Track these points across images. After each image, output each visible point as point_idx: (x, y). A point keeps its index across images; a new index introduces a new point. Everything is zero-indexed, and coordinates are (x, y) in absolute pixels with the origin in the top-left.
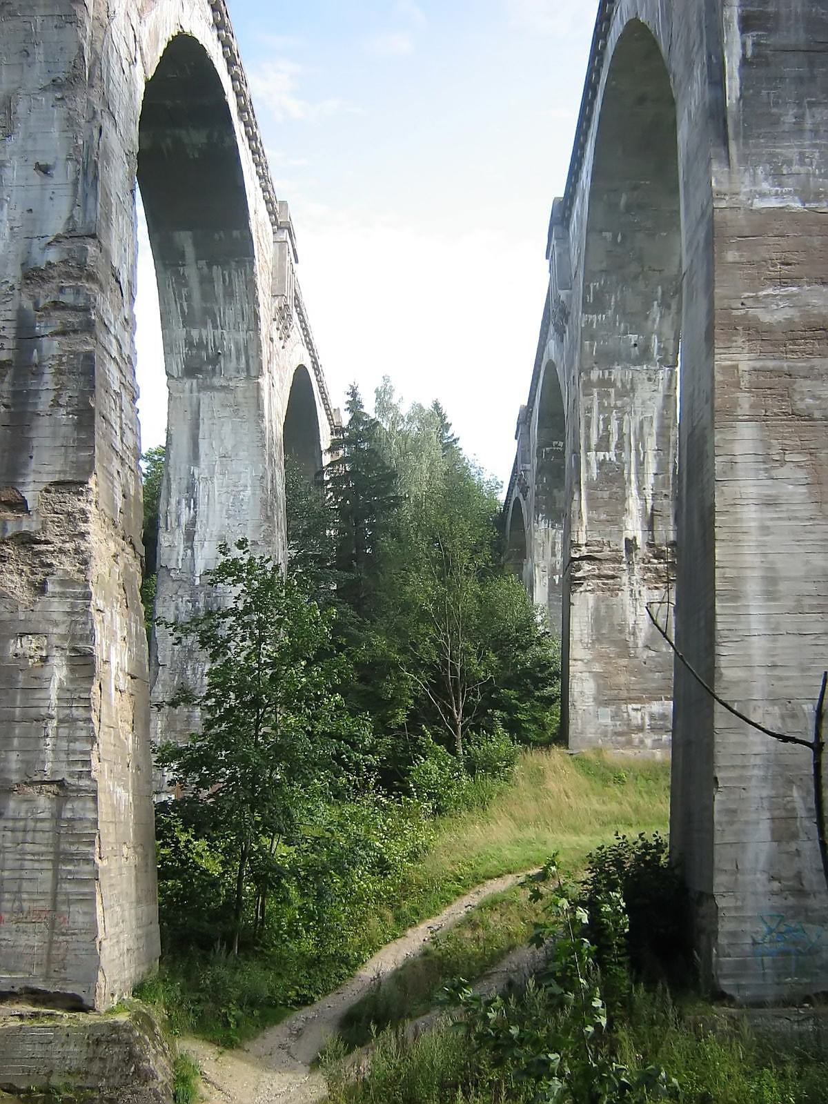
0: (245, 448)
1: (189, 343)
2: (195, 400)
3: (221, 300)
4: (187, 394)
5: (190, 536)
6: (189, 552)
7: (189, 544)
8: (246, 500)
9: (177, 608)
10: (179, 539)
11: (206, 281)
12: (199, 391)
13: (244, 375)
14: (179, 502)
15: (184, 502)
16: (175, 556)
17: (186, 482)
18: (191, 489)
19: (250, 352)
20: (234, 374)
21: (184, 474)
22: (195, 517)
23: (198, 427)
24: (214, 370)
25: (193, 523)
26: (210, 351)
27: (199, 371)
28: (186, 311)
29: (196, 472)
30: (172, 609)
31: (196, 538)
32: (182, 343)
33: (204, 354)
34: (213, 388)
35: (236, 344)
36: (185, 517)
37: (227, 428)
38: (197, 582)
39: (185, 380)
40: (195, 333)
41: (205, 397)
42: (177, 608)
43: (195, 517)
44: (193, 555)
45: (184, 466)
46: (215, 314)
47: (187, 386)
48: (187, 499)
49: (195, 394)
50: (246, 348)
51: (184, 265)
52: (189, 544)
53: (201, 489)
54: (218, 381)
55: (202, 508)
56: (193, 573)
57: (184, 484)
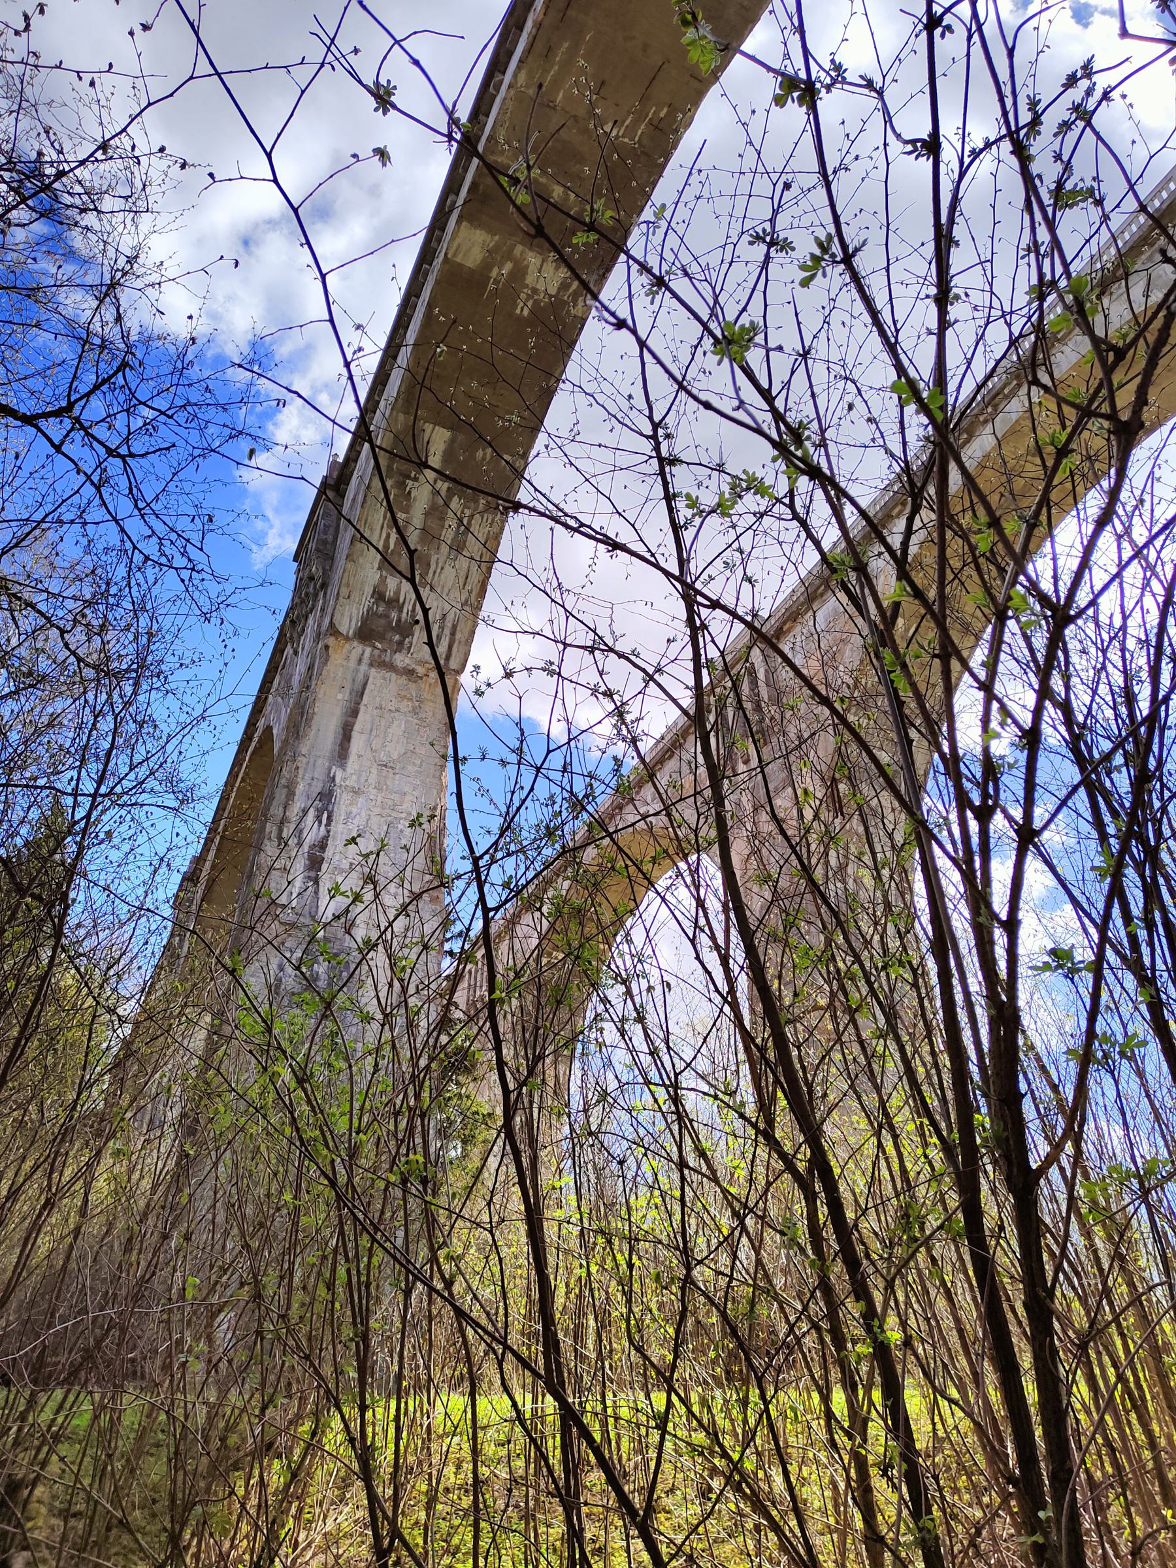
0: (418, 762)
1: (379, 595)
2: (361, 676)
3: (444, 549)
5: (315, 863)
7: (313, 874)
11: (436, 512)
12: (371, 665)
14: (305, 812)
15: (312, 813)
17: (320, 785)
18: (326, 797)
19: (458, 636)
21: (320, 773)
22: (326, 838)
23: (354, 713)
24: (400, 644)
25: (322, 845)
26: (404, 615)
27: (381, 638)
28: (392, 546)
31: (325, 866)
32: (369, 590)
33: (394, 615)
34: (390, 667)
36: (313, 832)
37: (397, 728)
39: (355, 643)
43: (326, 838)
45: (322, 763)
46: (429, 565)
47: (355, 655)
48: (317, 810)
49: (364, 667)
50: (454, 627)
51: (416, 479)
52: (313, 874)
53: (343, 803)
54: (401, 660)
57: (317, 787)
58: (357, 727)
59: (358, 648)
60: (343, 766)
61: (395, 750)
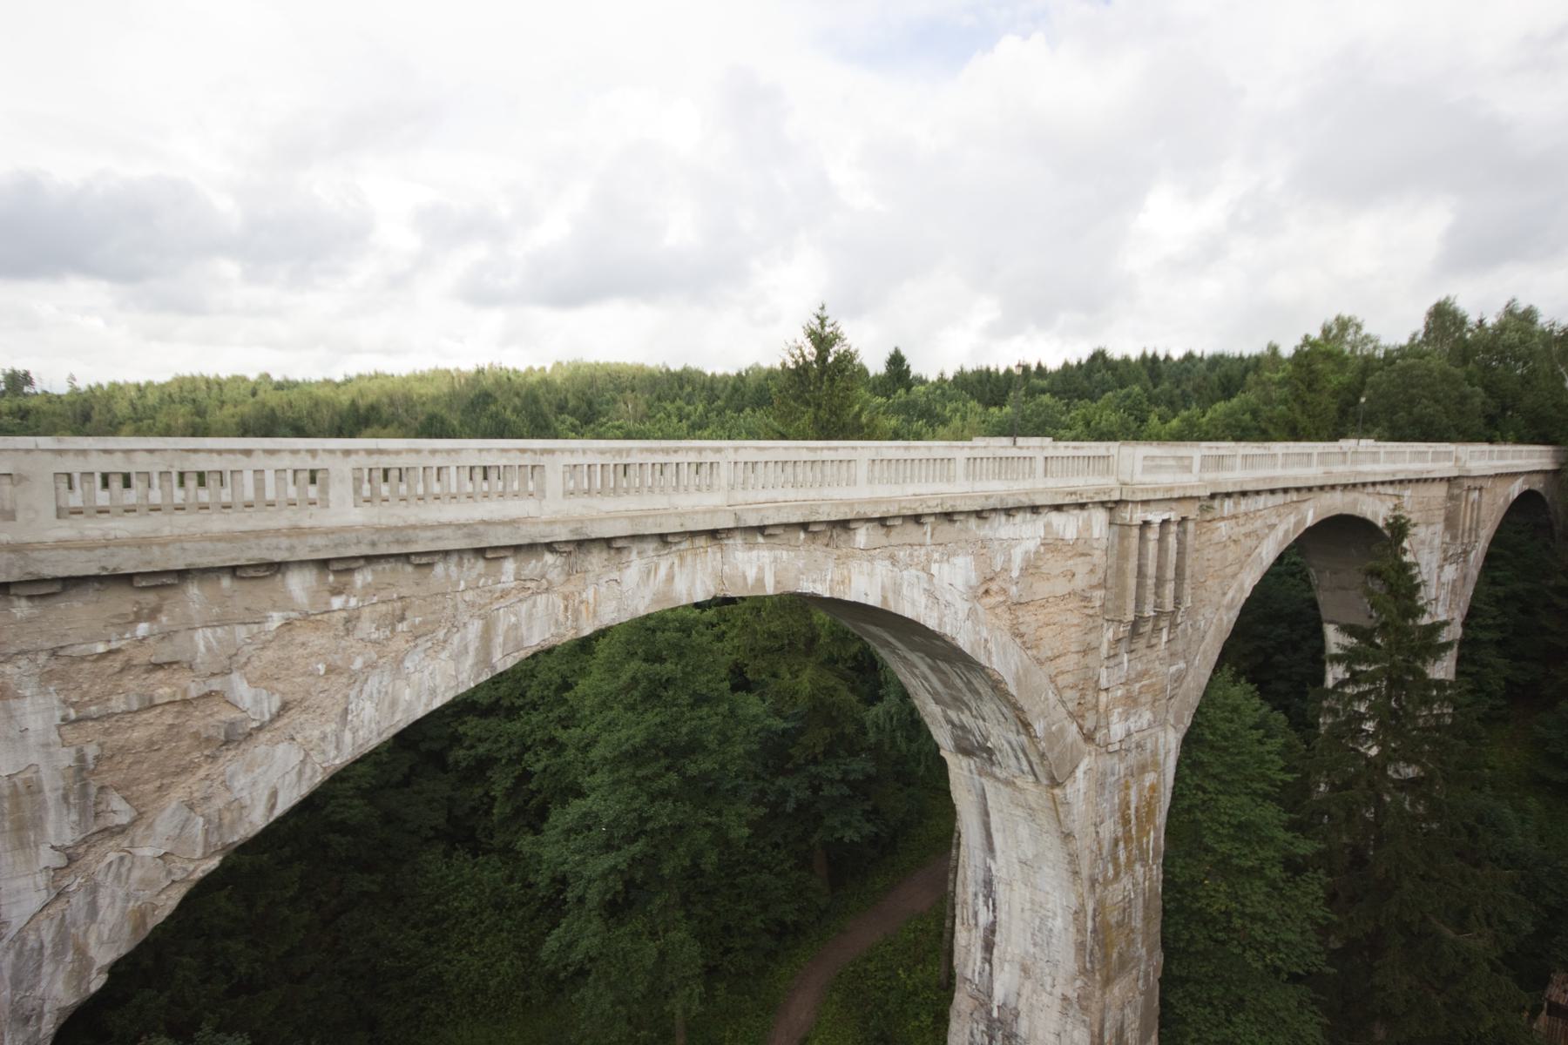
4: (966, 773)
5: (989, 947)
6: (987, 966)
8: (1056, 931)
9: (972, 1034)
10: (977, 937)
13: (1031, 778)
14: (976, 895)
15: (981, 898)
16: (971, 964)
18: (988, 883)
20: (1017, 773)
22: (994, 923)
23: (986, 814)
25: (991, 930)
29: (993, 868)
30: (967, 1032)
31: (995, 951)
34: (997, 779)
35: (1010, 743)
36: (984, 917)
37: (1024, 831)
38: (995, 1014)
40: (952, 714)
41: (989, 785)
42: (972, 1034)
43: (994, 923)
44: (991, 974)
53: (1000, 890)
55: (1002, 916)
56: (990, 996)
57: (980, 876)
58: (993, 826)
59: (965, 761)
60: (993, 858)
61: (1029, 851)
